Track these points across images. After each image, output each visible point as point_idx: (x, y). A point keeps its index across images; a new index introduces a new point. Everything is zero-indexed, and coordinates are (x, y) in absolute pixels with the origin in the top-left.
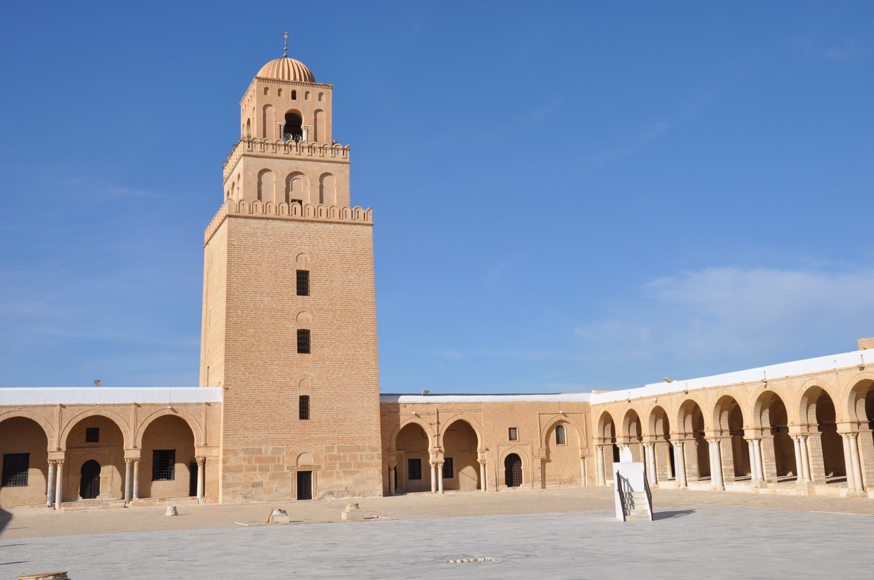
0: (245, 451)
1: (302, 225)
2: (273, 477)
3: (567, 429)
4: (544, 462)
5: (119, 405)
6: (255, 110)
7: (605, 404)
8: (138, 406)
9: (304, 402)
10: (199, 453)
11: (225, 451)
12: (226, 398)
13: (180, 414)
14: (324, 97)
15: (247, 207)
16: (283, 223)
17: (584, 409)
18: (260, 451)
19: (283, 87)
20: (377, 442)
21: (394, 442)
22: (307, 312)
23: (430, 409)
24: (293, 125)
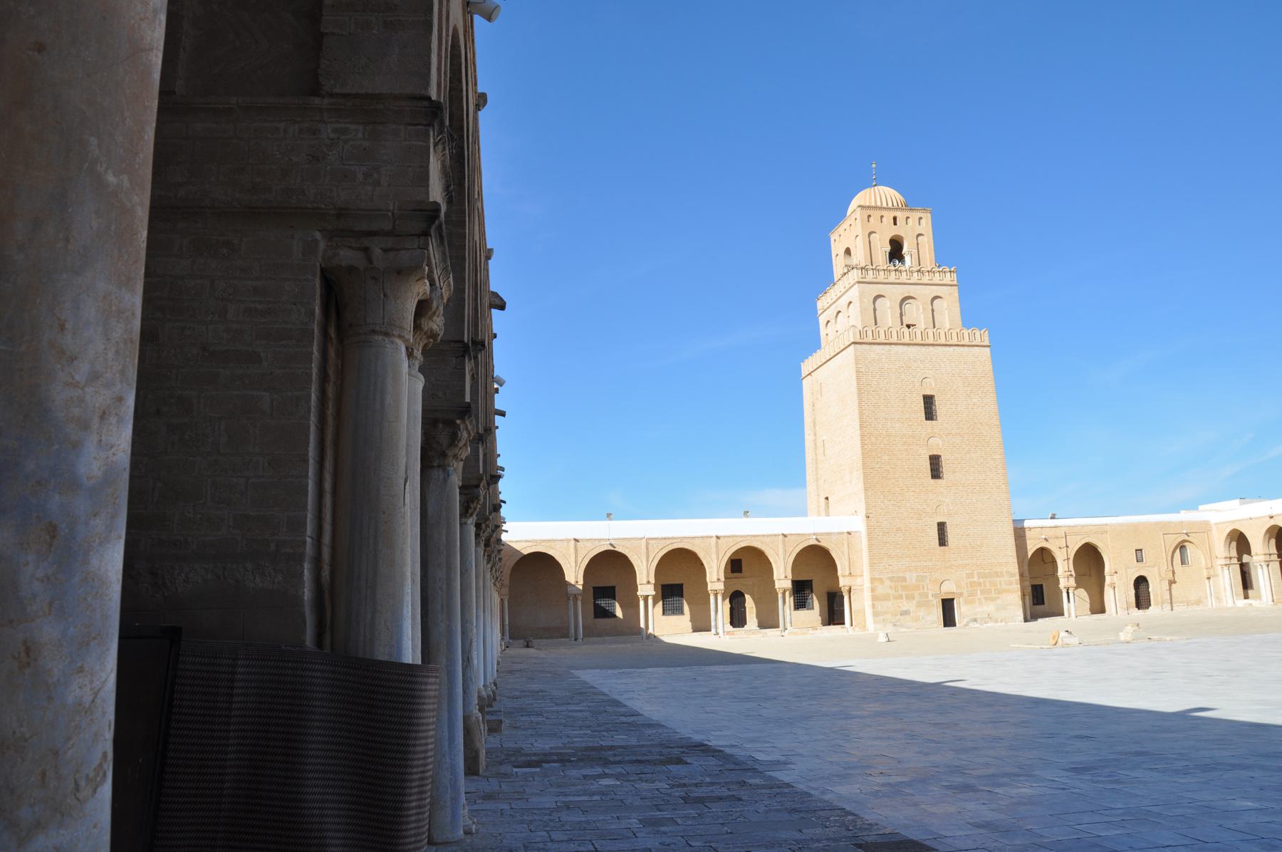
0: (891, 579)
1: (923, 349)
2: (919, 605)
3: (1190, 549)
4: (1172, 582)
5: (768, 536)
6: (853, 238)
7: (1233, 522)
8: (785, 536)
9: (942, 527)
10: (843, 582)
11: (873, 580)
12: (869, 527)
13: (823, 544)
14: (923, 221)
15: (870, 333)
16: (905, 348)
17: (1205, 528)
18: (904, 579)
19: (884, 213)
20: (1014, 569)
21: (1026, 568)
22: (937, 437)
23: (1060, 532)
24: (896, 251)
